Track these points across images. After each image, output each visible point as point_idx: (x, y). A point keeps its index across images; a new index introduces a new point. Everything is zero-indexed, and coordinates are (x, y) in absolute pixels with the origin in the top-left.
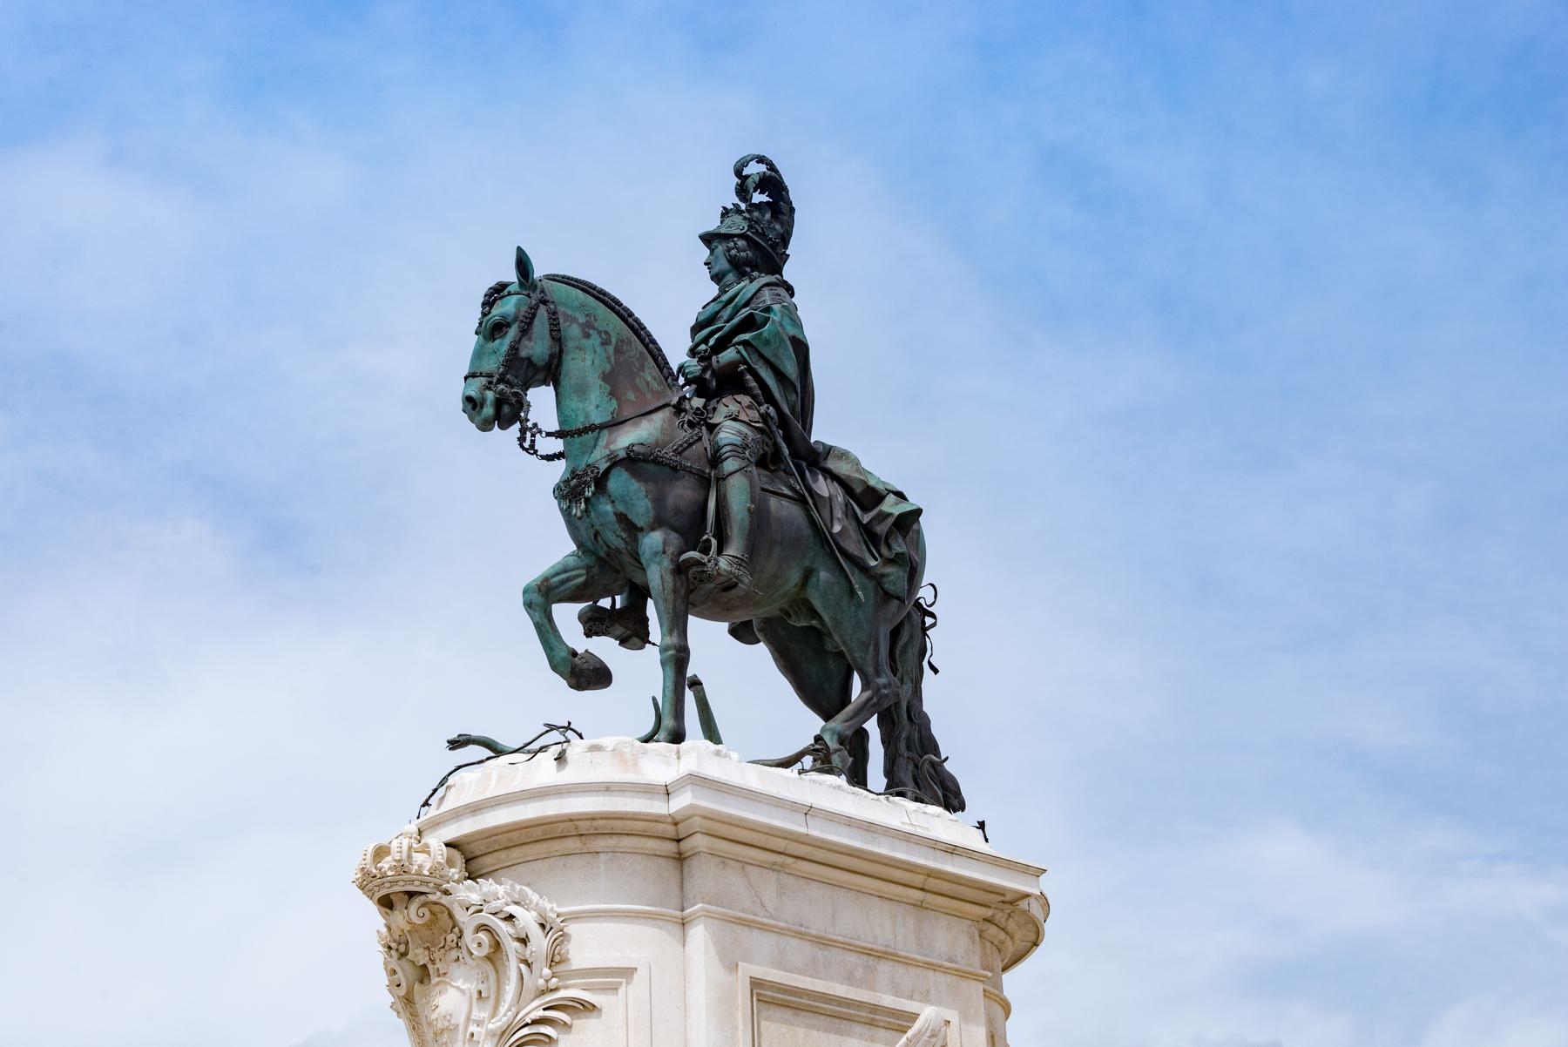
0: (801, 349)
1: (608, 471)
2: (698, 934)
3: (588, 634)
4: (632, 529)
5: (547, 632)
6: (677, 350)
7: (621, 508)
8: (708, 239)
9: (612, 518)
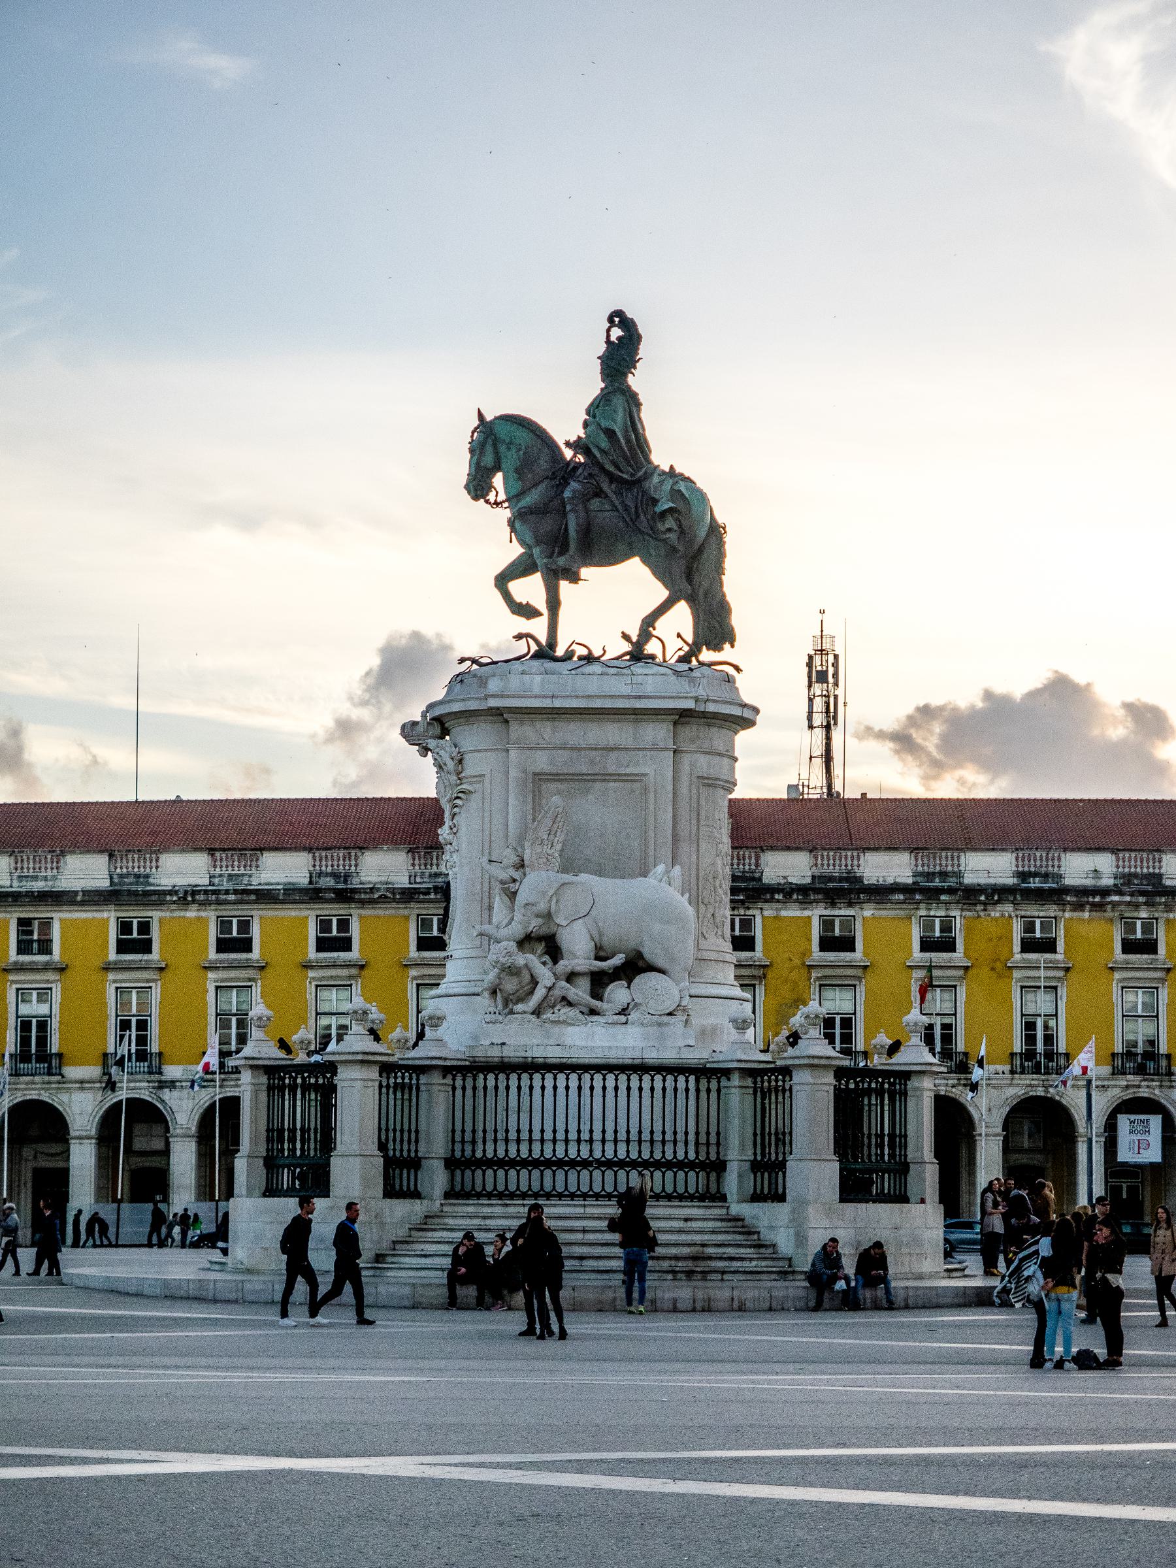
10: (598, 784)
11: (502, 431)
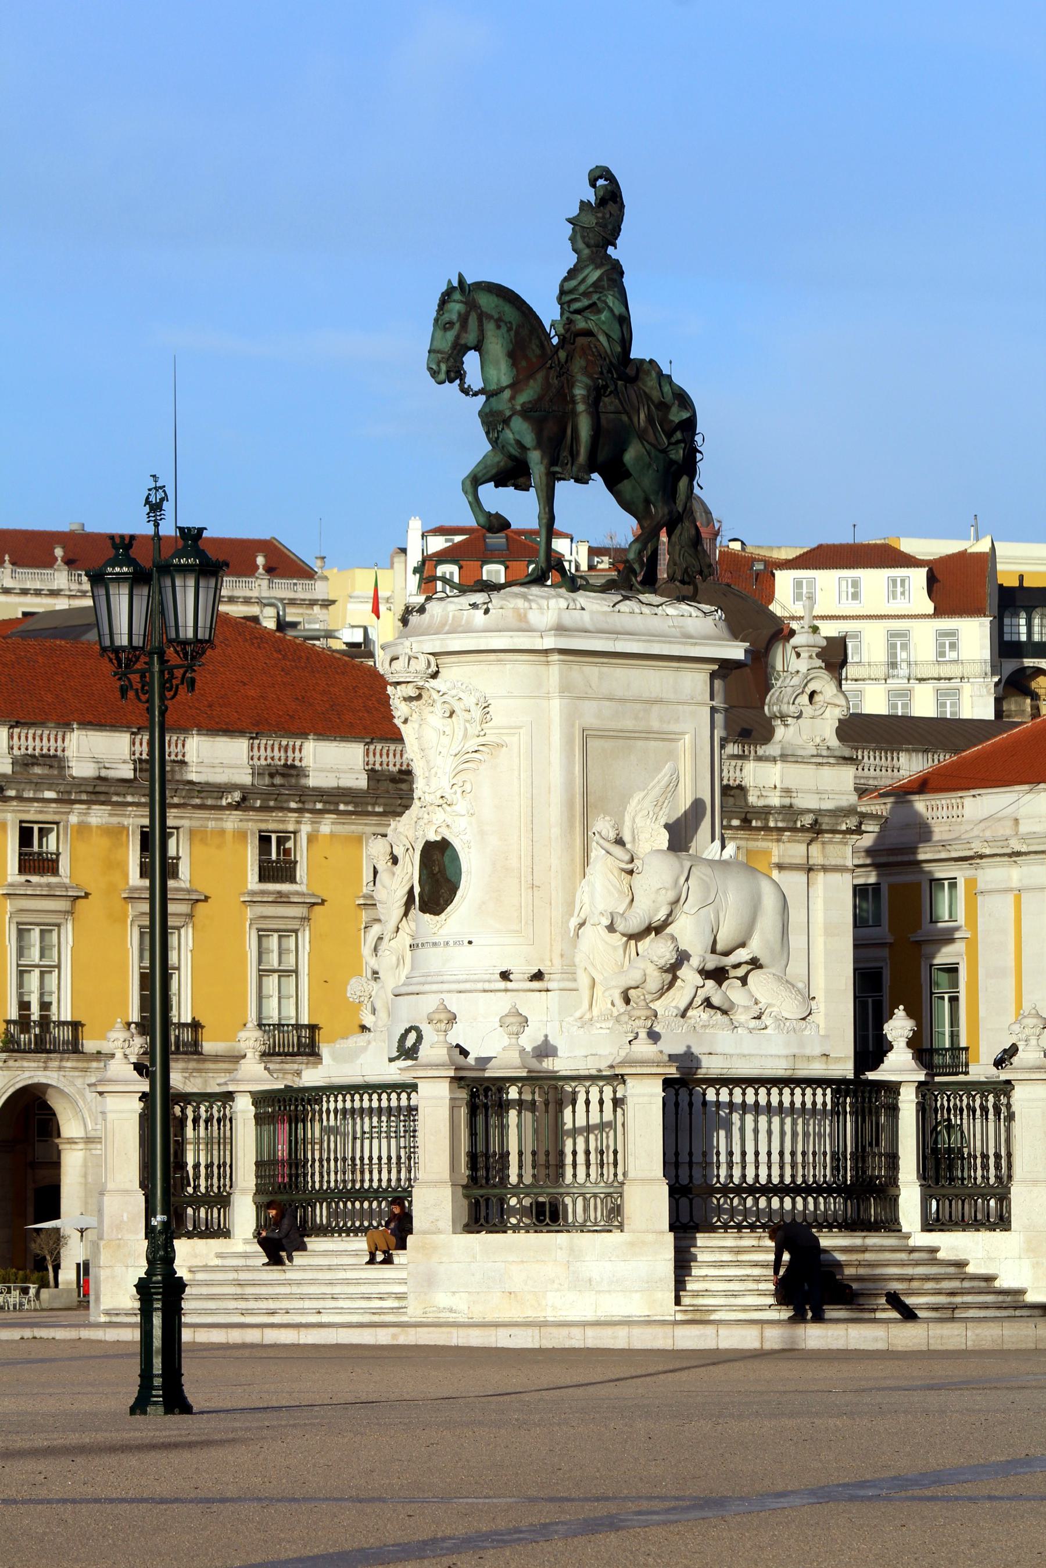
0: (624, 321)
1: (510, 417)
6: (548, 312)
7: (518, 437)
8: (570, 221)
9: (513, 442)
10: (640, 743)
11: (485, 301)
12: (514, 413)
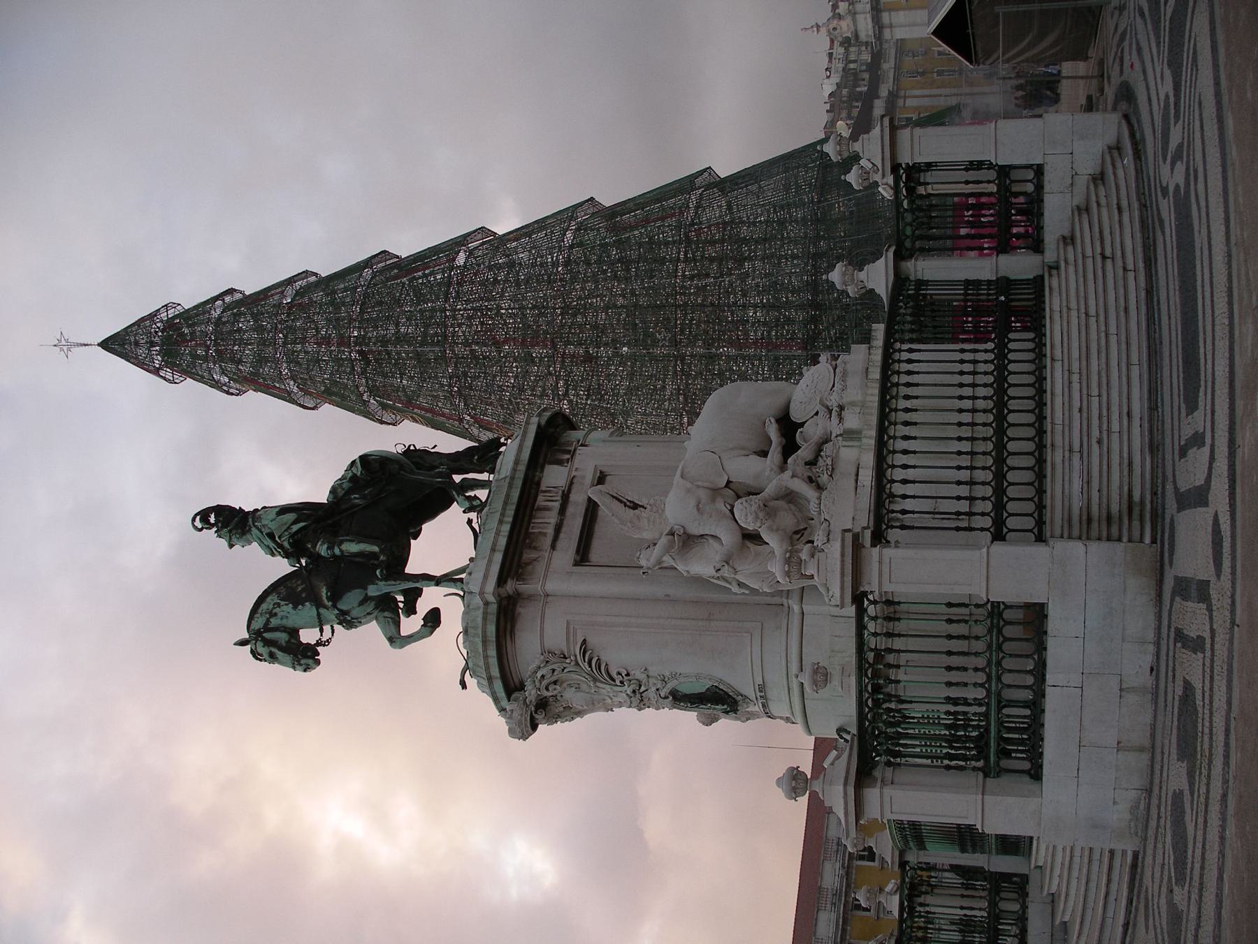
2: (552, 586)
3: (415, 613)
4: (366, 599)
5: (412, 638)
8: (231, 546)
11: (258, 623)
12: (335, 606)
